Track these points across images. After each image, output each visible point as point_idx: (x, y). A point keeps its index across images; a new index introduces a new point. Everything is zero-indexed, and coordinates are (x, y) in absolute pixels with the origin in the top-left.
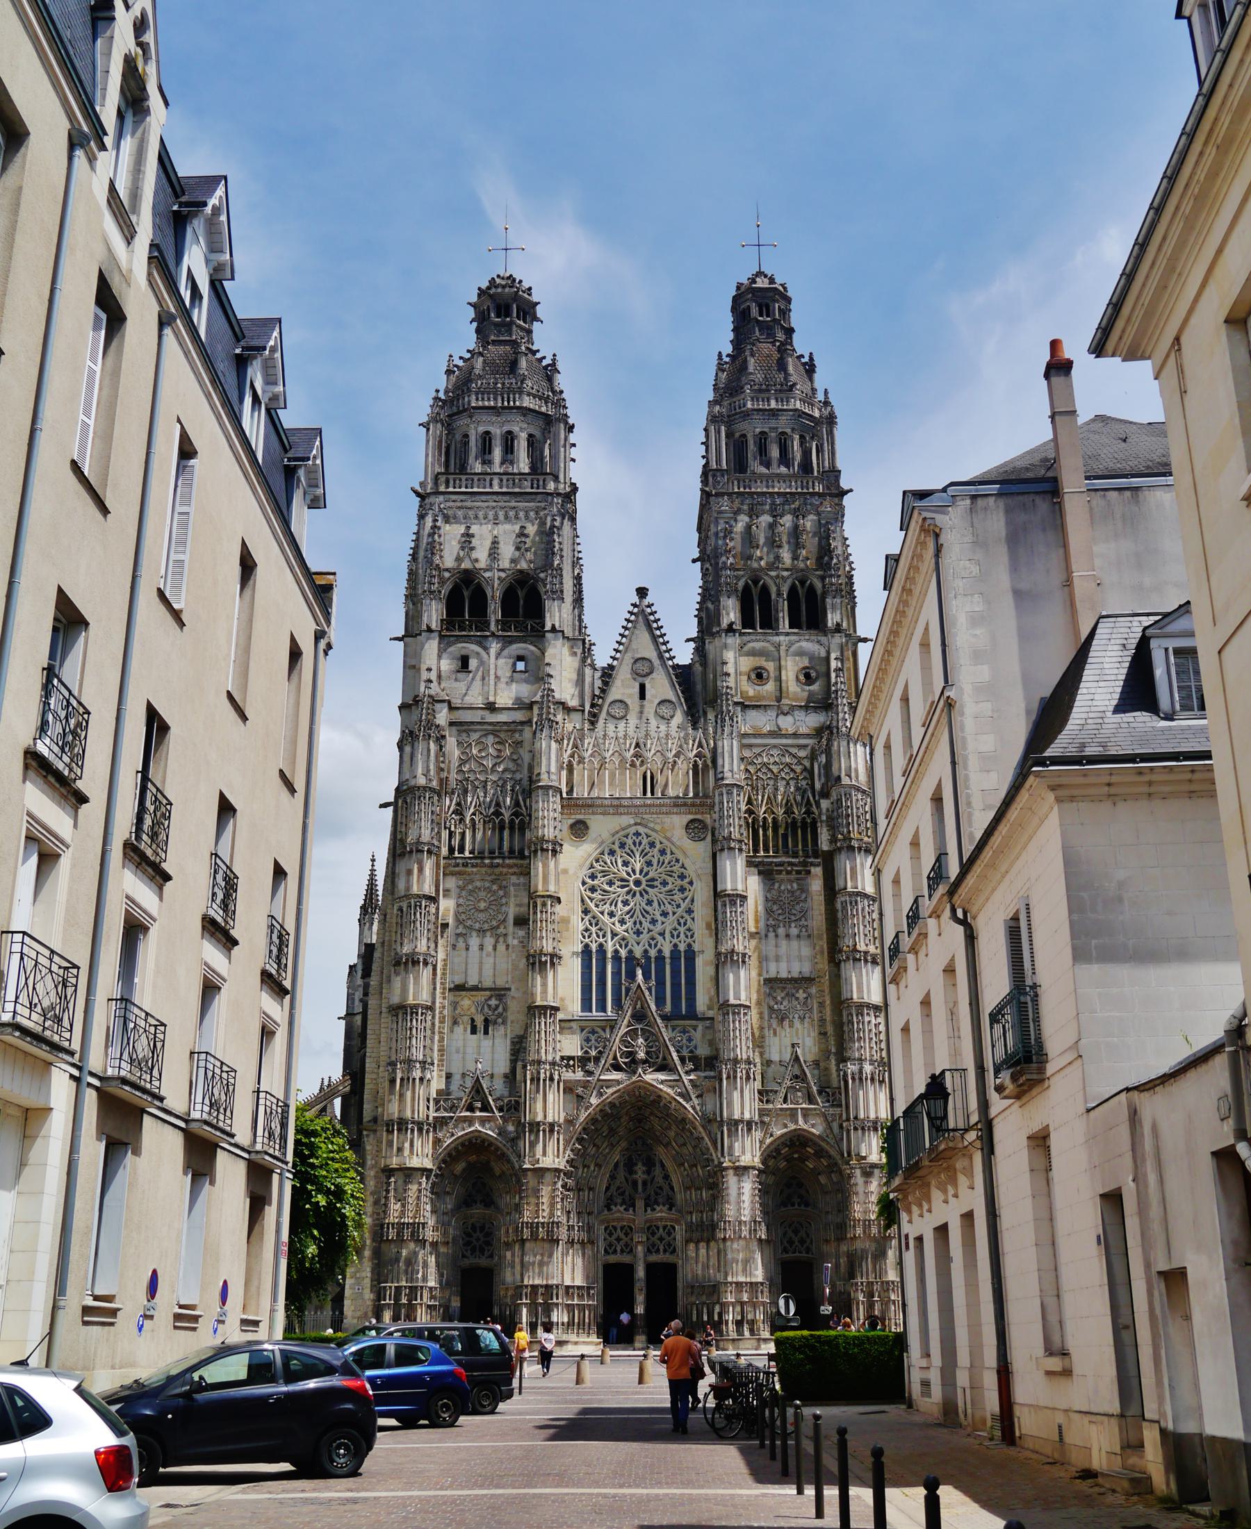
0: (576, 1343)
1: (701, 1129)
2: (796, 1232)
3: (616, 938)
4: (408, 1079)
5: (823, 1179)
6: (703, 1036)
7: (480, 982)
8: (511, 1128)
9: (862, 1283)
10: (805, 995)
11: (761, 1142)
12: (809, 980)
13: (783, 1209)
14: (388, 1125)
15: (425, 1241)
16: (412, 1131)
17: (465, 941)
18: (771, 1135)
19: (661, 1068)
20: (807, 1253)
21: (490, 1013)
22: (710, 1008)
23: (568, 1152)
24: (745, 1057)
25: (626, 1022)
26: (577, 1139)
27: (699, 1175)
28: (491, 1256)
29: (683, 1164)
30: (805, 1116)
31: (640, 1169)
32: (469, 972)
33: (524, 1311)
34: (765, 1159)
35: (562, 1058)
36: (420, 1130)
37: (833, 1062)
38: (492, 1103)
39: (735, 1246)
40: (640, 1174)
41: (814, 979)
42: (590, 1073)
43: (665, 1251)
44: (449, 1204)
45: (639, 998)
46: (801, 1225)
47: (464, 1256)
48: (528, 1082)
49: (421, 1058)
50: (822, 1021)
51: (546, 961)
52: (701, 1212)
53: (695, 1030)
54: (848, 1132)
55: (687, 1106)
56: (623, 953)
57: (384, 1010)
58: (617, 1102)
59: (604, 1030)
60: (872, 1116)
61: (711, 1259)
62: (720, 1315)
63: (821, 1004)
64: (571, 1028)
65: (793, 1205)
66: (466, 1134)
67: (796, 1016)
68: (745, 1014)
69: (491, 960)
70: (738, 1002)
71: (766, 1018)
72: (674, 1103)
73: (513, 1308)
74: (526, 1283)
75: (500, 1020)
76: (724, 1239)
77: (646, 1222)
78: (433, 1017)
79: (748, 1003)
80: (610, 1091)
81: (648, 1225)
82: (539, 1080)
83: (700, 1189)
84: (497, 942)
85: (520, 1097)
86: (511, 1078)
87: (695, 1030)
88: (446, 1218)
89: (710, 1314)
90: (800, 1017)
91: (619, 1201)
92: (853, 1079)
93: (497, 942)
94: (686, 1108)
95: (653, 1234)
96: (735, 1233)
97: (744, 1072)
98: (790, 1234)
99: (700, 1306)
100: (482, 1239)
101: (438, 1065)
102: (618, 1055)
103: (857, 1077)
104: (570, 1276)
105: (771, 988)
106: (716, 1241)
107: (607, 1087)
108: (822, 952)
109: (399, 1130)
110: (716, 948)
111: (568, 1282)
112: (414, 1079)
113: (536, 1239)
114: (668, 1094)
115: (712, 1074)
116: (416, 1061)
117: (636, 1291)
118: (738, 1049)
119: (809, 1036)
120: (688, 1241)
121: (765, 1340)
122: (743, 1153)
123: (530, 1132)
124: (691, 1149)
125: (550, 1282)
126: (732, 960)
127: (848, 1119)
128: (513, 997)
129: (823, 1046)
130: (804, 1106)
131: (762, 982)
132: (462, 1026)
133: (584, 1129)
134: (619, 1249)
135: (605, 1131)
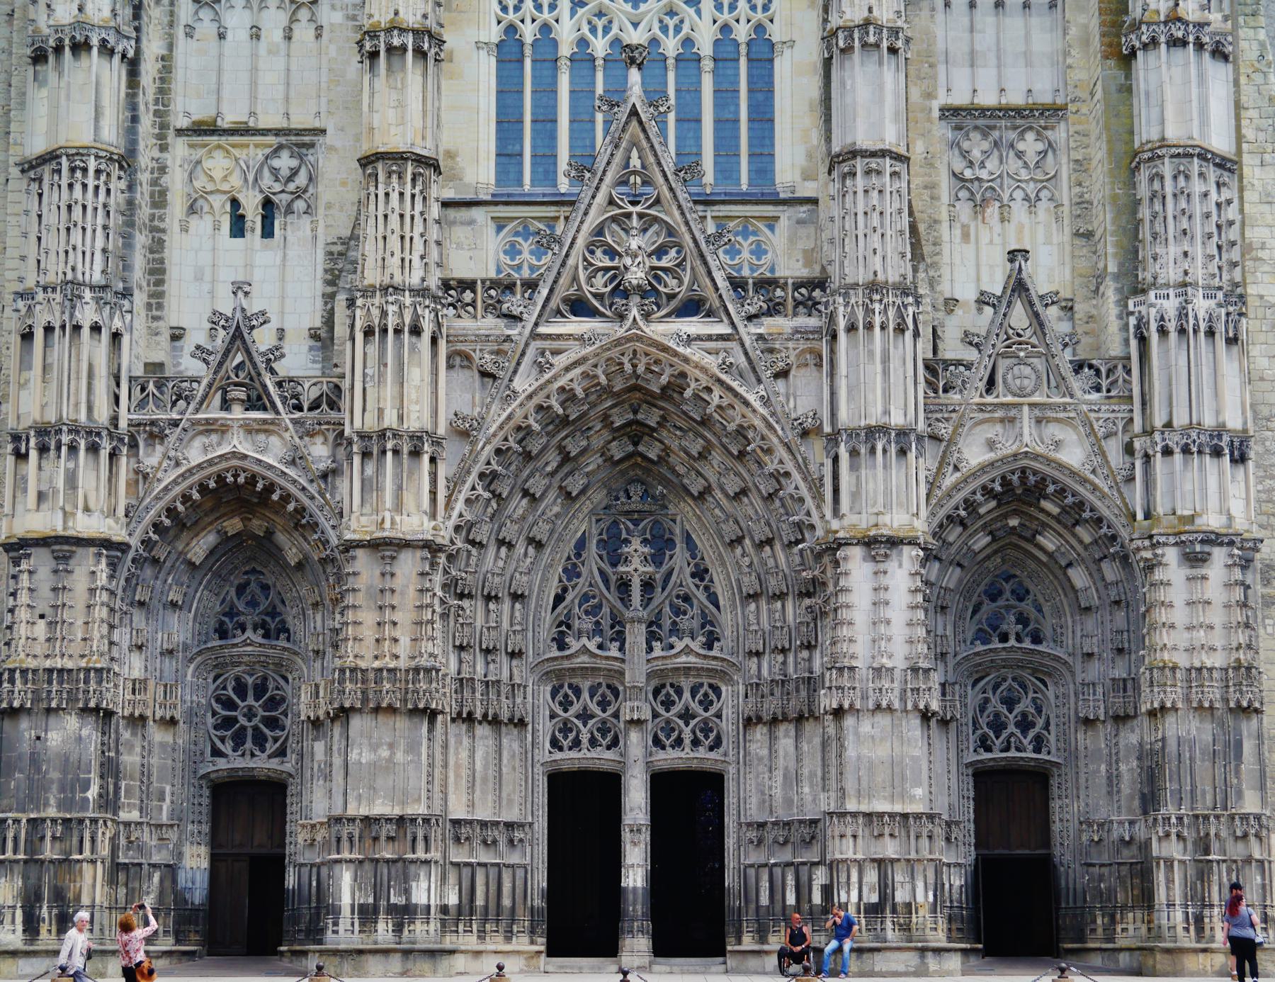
0: (477, 954)
1: (781, 452)
2: (1010, 703)
3: (581, 11)
4: (63, 327)
5: (1079, 577)
6: (792, 240)
7: (252, 114)
8: (320, 451)
9: (1180, 819)
10: (1040, 146)
11: (932, 485)
12: (1054, 111)
13: (980, 648)
14: (16, 438)
15: (109, 714)
16: (73, 448)
17: (217, 19)
18: (956, 468)
19: (692, 307)
20: (1037, 750)
21: (277, 187)
22: (807, 177)
23: (459, 506)
24: (893, 277)
25: (601, 198)
26: (482, 476)
27: (777, 567)
28: (281, 753)
29: (739, 540)
30: (1039, 421)
31: (636, 548)
32: (226, 93)
33: (346, 878)
34: (941, 526)
35: (446, 285)
36: (94, 449)
37: (1110, 292)
38: (271, 388)
39: (866, 726)
40: (636, 566)
41: (1064, 108)
42: (515, 318)
43: (696, 743)
44: (179, 629)
45: (634, 144)
46: (1023, 686)
47: (216, 753)
48: (359, 337)
49: (97, 278)
50: (1083, 204)
51: (404, 49)
52: (783, 651)
53: (771, 228)
54: (1147, 458)
55: (751, 398)
56: (600, 47)
57: (15, 172)
58: (580, 392)
59: (552, 228)
60: (1209, 421)
61: (806, 761)
62: (827, 891)
63: (1080, 165)
64: (471, 222)
65: (1004, 638)
66: (210, 462)
67: (1019, 195)
68: (895, 174)
69: (280, 63)
70: (879, 146)
71: (945, 198)
72: (717, 392)
73: (324, 871)
74: (352, 811)
75: (300, 205)
76: (838, 713)
77: (650, 676)
78: (131, 187)
79: (902, 150)
80: (560, 361)
81: (655, 682)
82: (384, 331)
83: (781, 596)
84: (293, 20)
85: (343, 376)
86: (323, 338)
87: (771, 228)
88: (169, 665)
89: (802, 890)
90: (1027, 198)
91: (587, 624)
92: (1163, 332)
93: (293, 20)
94: (746, 403)
95: (668, 704)
96: (865, 697)
97: (891, 313)
98: (996, 704)
99: (778, 871)
100: (261, 712)
101: (149, 306)
102: (582, 276)
103: (1172, 326)
104: (464, 799)
105: (958, 128)
106: (817, 718)
107: (556, 353)
108: (1086, 42)
109: (43, 449)
110: (825, 21)
111: (458, 810)
112: (77, 328)
113: (377, 710)
114: (704, 370)
115: (813, 322)
116: (84, 284)
117: (626, 836)
118: (878, 259)
119: (1048, 242)
120: (748, 722)
121: (938, 951)
122: (888, 506)
123: (366, 455)
124: (758, 503)
125: (410, 811)
126: (865, 45)
127: (1148, 432)
128: (331, 148)
129: (1083, 264)
130: (1036, 398)
131: (936, 114)
132: (208, 219)
133: (498, 452)
134: (585, 738)
135: (553, 459)
